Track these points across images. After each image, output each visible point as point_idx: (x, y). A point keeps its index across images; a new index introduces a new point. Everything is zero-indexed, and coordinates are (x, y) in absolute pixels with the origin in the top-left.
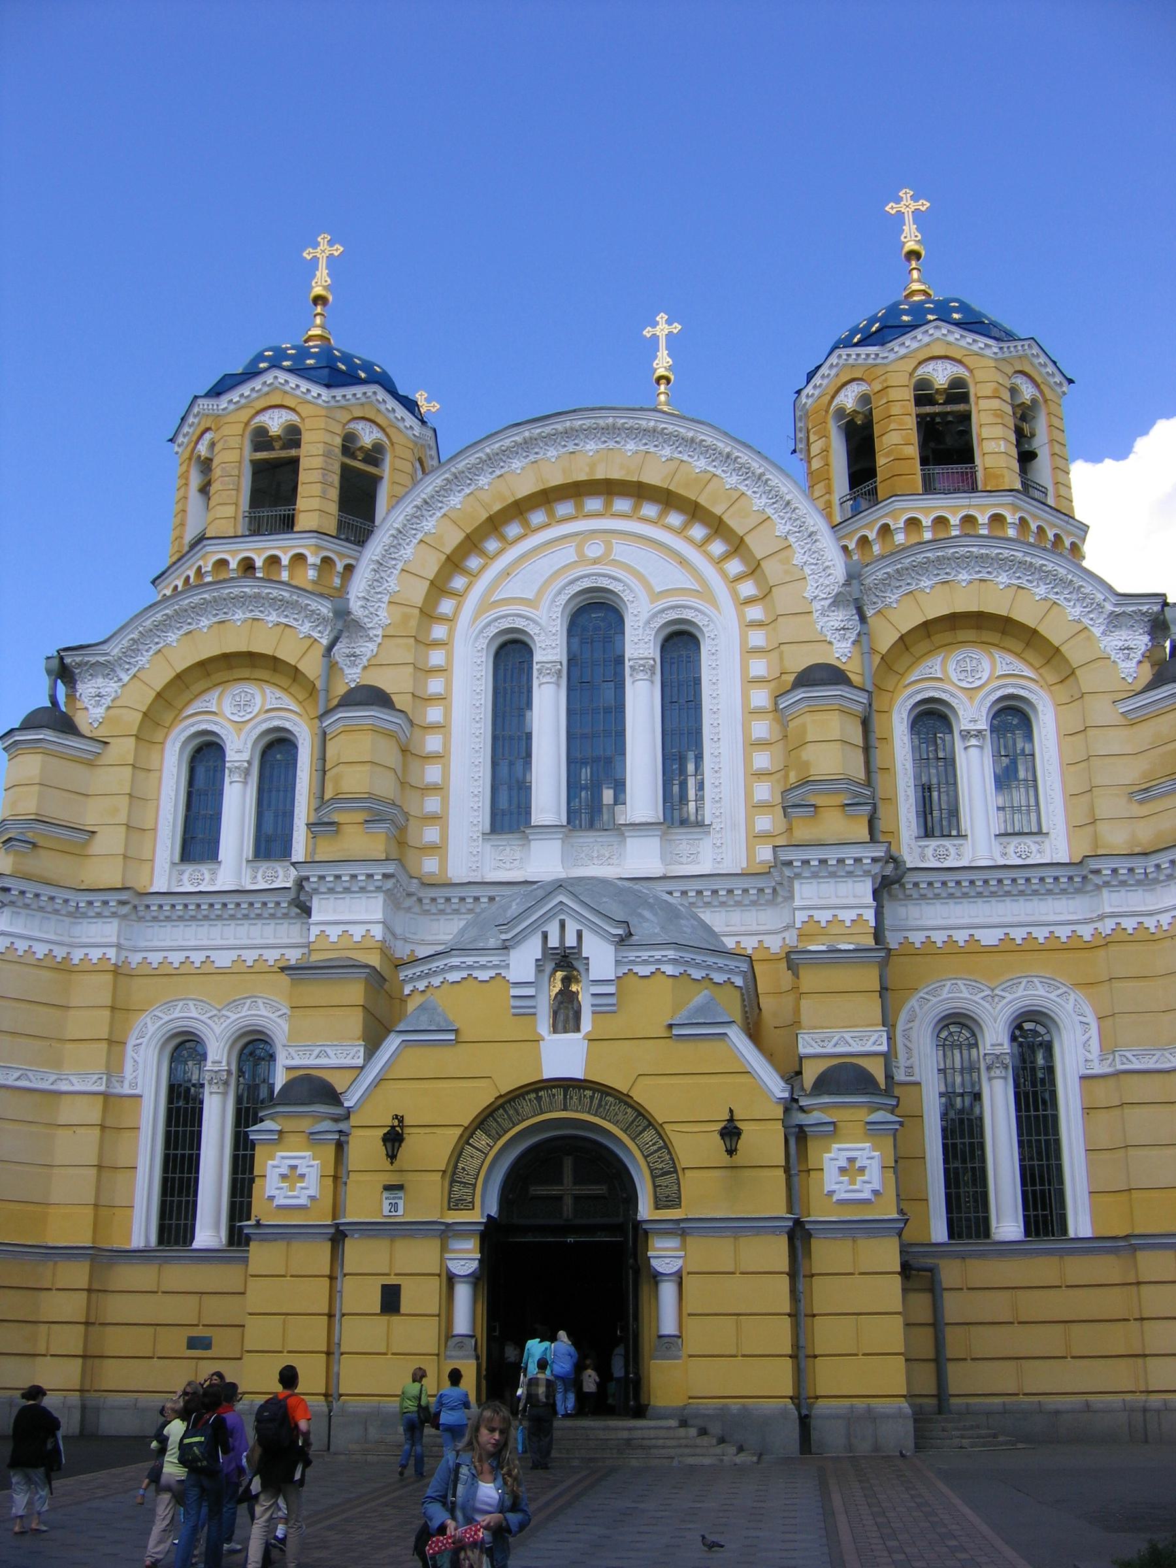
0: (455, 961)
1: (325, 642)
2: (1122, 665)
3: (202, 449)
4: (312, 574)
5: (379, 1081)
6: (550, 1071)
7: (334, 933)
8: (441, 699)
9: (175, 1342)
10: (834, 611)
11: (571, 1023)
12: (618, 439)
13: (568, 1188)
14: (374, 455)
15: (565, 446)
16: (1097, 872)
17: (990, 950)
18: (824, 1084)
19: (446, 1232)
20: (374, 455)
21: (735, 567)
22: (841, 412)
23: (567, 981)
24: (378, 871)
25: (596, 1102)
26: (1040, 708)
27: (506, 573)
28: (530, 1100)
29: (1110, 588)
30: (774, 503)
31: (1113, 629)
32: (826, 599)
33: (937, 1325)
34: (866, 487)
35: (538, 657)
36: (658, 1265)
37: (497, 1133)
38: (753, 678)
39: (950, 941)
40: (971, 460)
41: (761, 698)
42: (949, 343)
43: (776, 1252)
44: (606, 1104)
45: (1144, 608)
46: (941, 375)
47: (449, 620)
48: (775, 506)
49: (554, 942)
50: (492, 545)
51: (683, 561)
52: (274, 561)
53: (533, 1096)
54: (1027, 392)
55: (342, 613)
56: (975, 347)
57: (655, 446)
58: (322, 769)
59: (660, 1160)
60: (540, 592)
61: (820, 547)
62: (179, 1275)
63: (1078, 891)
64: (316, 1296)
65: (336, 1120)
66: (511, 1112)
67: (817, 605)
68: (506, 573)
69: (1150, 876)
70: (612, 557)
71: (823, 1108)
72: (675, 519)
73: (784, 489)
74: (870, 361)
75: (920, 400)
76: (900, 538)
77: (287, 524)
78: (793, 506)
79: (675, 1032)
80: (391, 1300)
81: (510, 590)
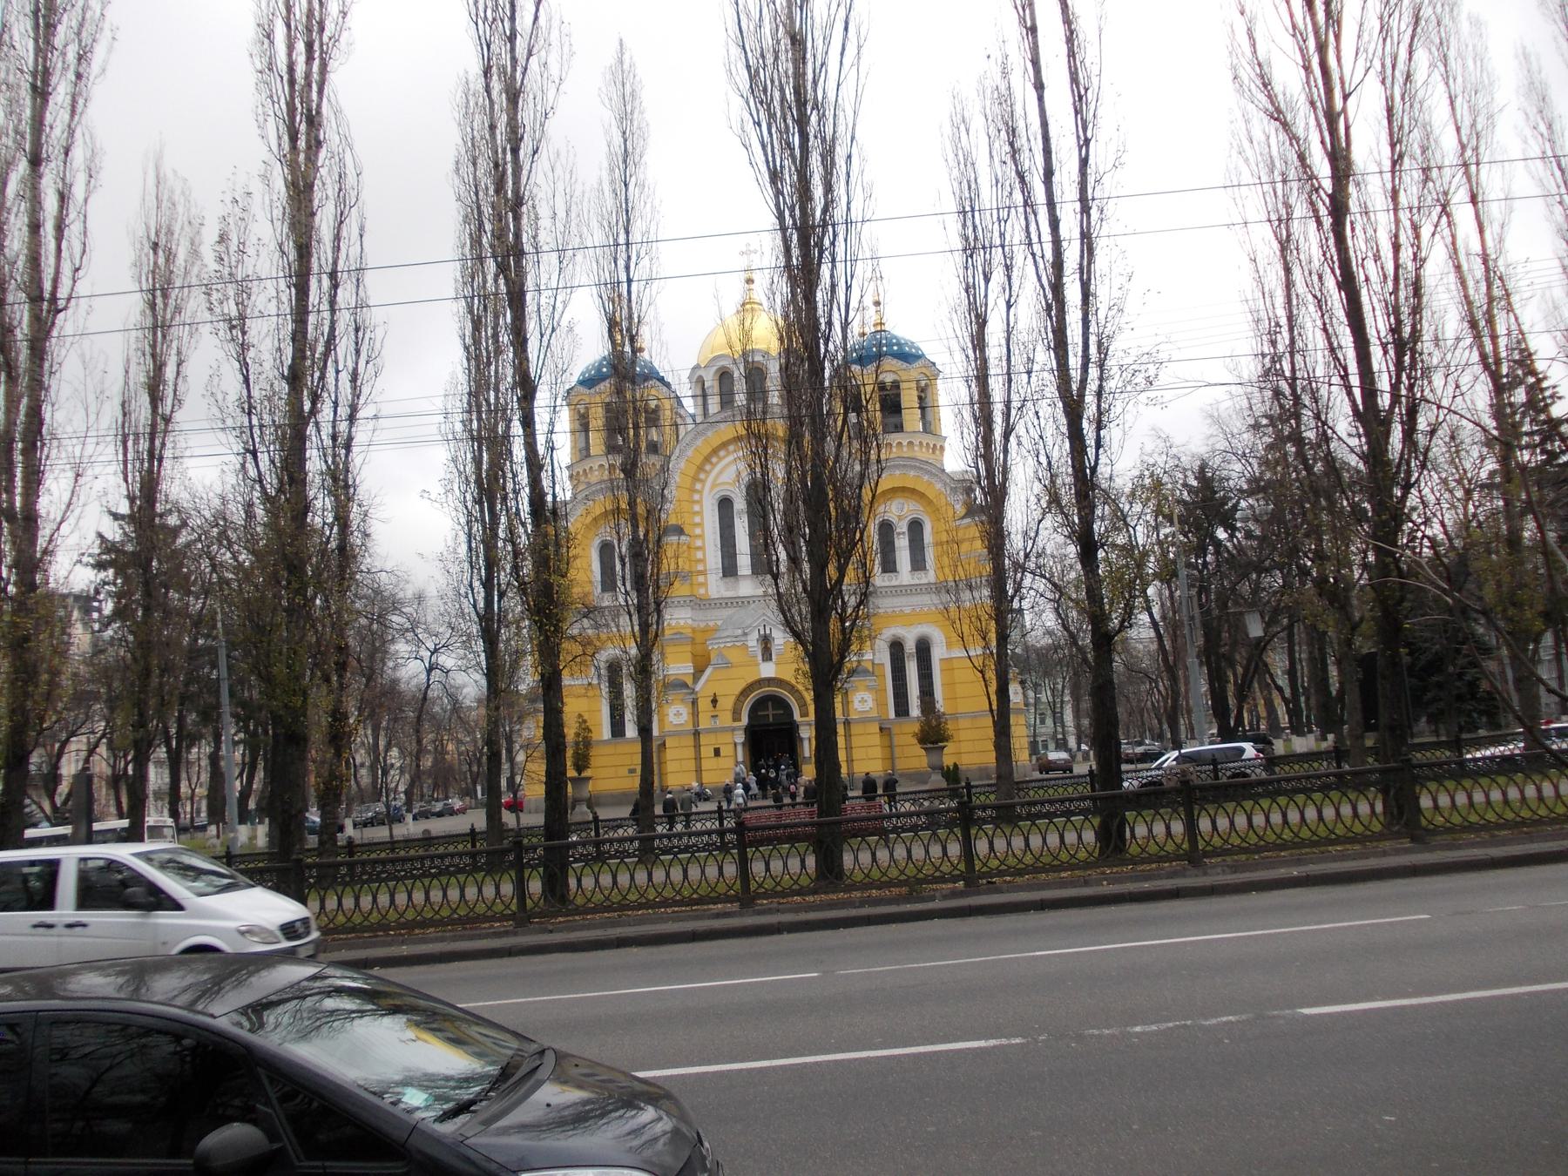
5: (707, 681)
6: (764, 675)
8: (700, 525)
9: (625, 771)
23: (766, 644)
24: (688, 599)
27: (721, 472)
33: (891, 747)
36: (802, 735)
47: (700, 492)
49: (762, 632)
50: (714, 460)
62: (622, 748)
64: (691, 753)
68: (721, 472)
80: (717, 752)
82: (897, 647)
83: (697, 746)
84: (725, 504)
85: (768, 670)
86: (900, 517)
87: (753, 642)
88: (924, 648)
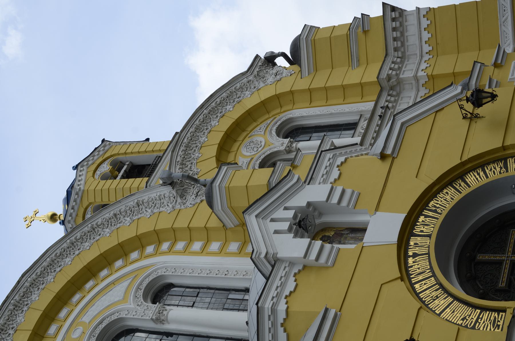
0: (268, 305)
2: (284, 75)
6: (394, 238)
10: (185, 198)
11: (359, 235)
12: (26, 303)
15: (10, 334)
16: (389, 78)
25: (431, 214)
26: (291, 116)
28: (414, 262)
29: (243, 74)
30: (111, 225)
31: (264, 79)
32: (176, 201)
37: (437, 290)
38: (201, 249)
42: (93, 164)
44: (435, 206)
45: (260, 64)
48: (113, 224)
49: (285, 226)
51: (113, 283)
53: (411, 260)
56: (101, 153)
57: (43, 284)
59: (493, 169)
61: (146, 199)
63: (398, 95)
66: (420, 278)
67: (178, 207)
69: (400, 55)
70: (87, 322)
73: (107, 215)
74: (78, 200)
78: (118, 213)
79: (389, 152)
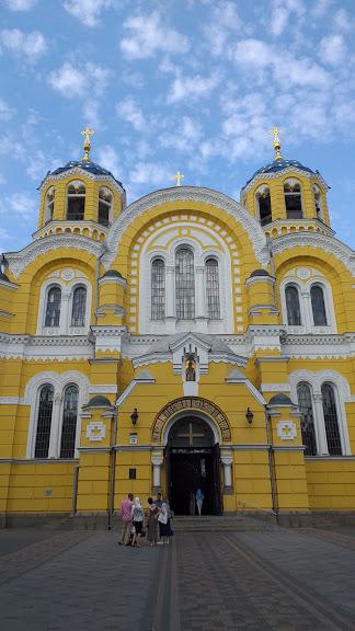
0: (154, 356)
1: (98, 256)
3: (50, 192)
4: (90, 235)
5: (127, 397)
7: (104, 349)
13: (191, 435)
14: (108, 200)
17: (314, 362)
18: (273, 400)
19: (152, 449)
20: (108, 200)
21: (229, 239)
22: (258, 194)
23: (190, 364)
24: (119, 329)
27: (157, 238)
34: (267, 218)
35: (166, 265)
36: (224, 461)
39: (300, 358)
40: (300, 209)
41: (238, 280)
43: (264, 457)
46: (292, 183)
49: (188, 351)
51: (212, 236)
52: (77, 230)
54: (317, 190)
55: (105, 247)
58: (97, 296)
60: (168, 244)
62: (43, 468)
65: (112, 410)
68: (157, 238)
71: (275, 408)
72: (210, 223)
75: (286, 190)
76: (280, 233)
77: (82, 218)
80: (133, 474)
81: (159, 242)
82: (304, 387)
83: (113, 467)
84: (158, 262)
85: (191, 389)
86: (305, 281)
87: (177, 357)
88: (328, 388)
